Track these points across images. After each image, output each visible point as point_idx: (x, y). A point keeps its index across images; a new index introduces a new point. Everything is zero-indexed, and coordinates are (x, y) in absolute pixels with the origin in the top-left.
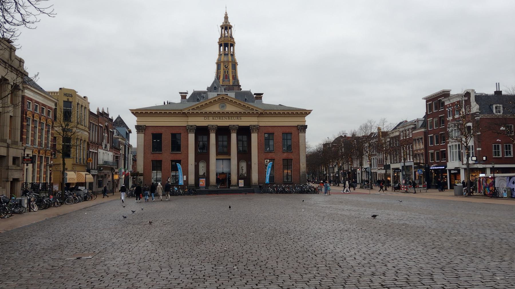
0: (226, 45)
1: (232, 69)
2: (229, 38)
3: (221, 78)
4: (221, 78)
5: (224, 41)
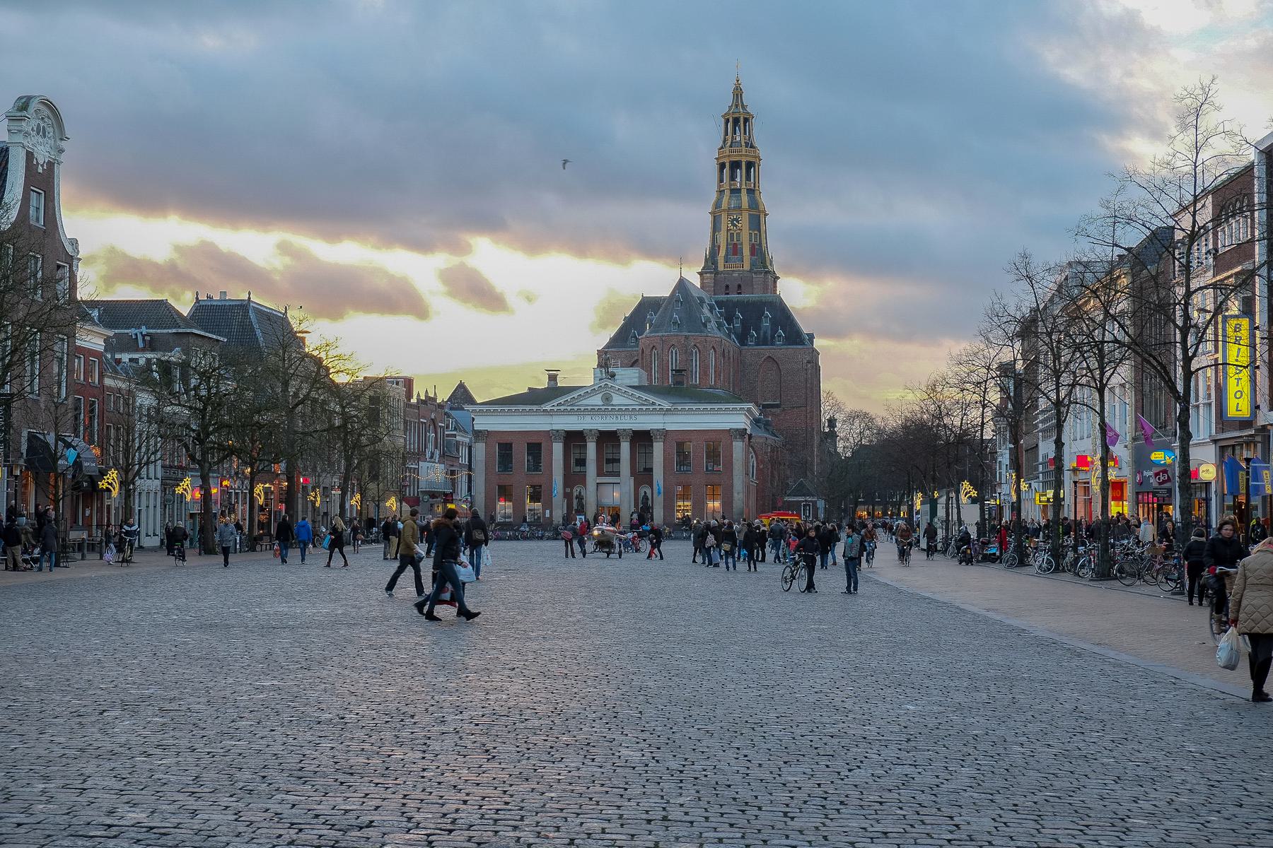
0: (735, 165)
1: (749, 230)
2: (744, 148)
3: (722, 253)
4: (722, 253)
5: (729, 156)
